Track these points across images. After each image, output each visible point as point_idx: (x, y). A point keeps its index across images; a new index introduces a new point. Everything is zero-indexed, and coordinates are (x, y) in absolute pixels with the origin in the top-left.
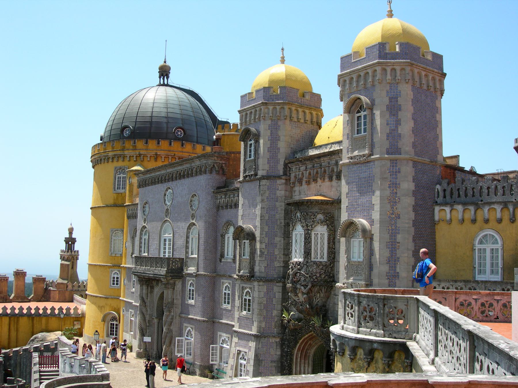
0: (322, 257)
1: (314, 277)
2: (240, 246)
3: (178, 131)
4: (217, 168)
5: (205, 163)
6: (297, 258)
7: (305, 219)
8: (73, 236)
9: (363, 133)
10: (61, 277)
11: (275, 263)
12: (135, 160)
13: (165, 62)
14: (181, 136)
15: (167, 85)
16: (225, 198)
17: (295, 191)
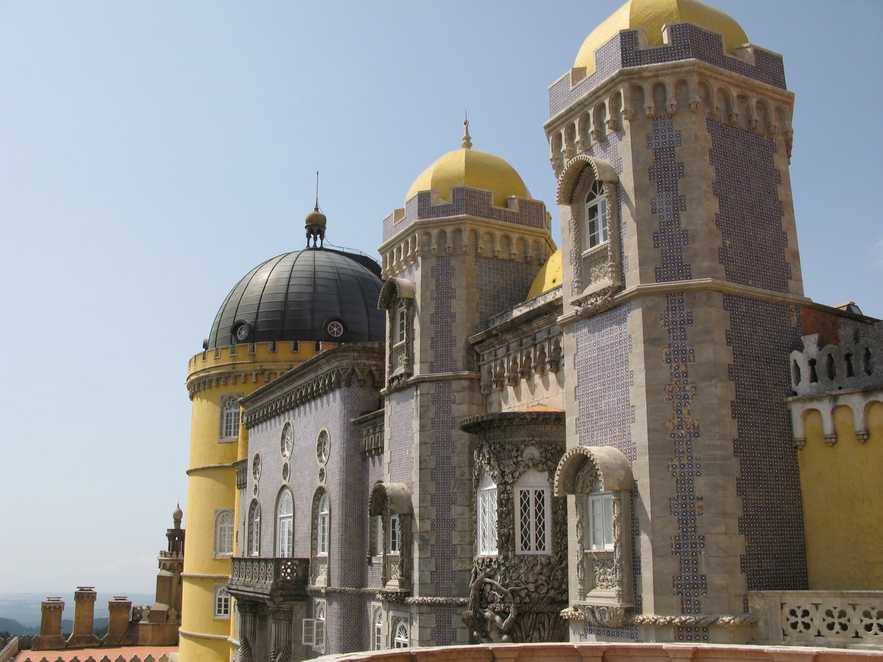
0: (540, 545)
1: (523, 593)
2: (384, 528)
3: (333, 325)
4: (359, 374)
5: (337, 367)
6: (488, 549)
7: (499, 461)
8: (182, 527)
9: (602, 242)
10: (159, 599)
11: (454, 562)
12: (254, 380)
13: (317, 209)
14: (338, 334)
15: (321, 249)
16: (374, 434)
17: (491, 404)
